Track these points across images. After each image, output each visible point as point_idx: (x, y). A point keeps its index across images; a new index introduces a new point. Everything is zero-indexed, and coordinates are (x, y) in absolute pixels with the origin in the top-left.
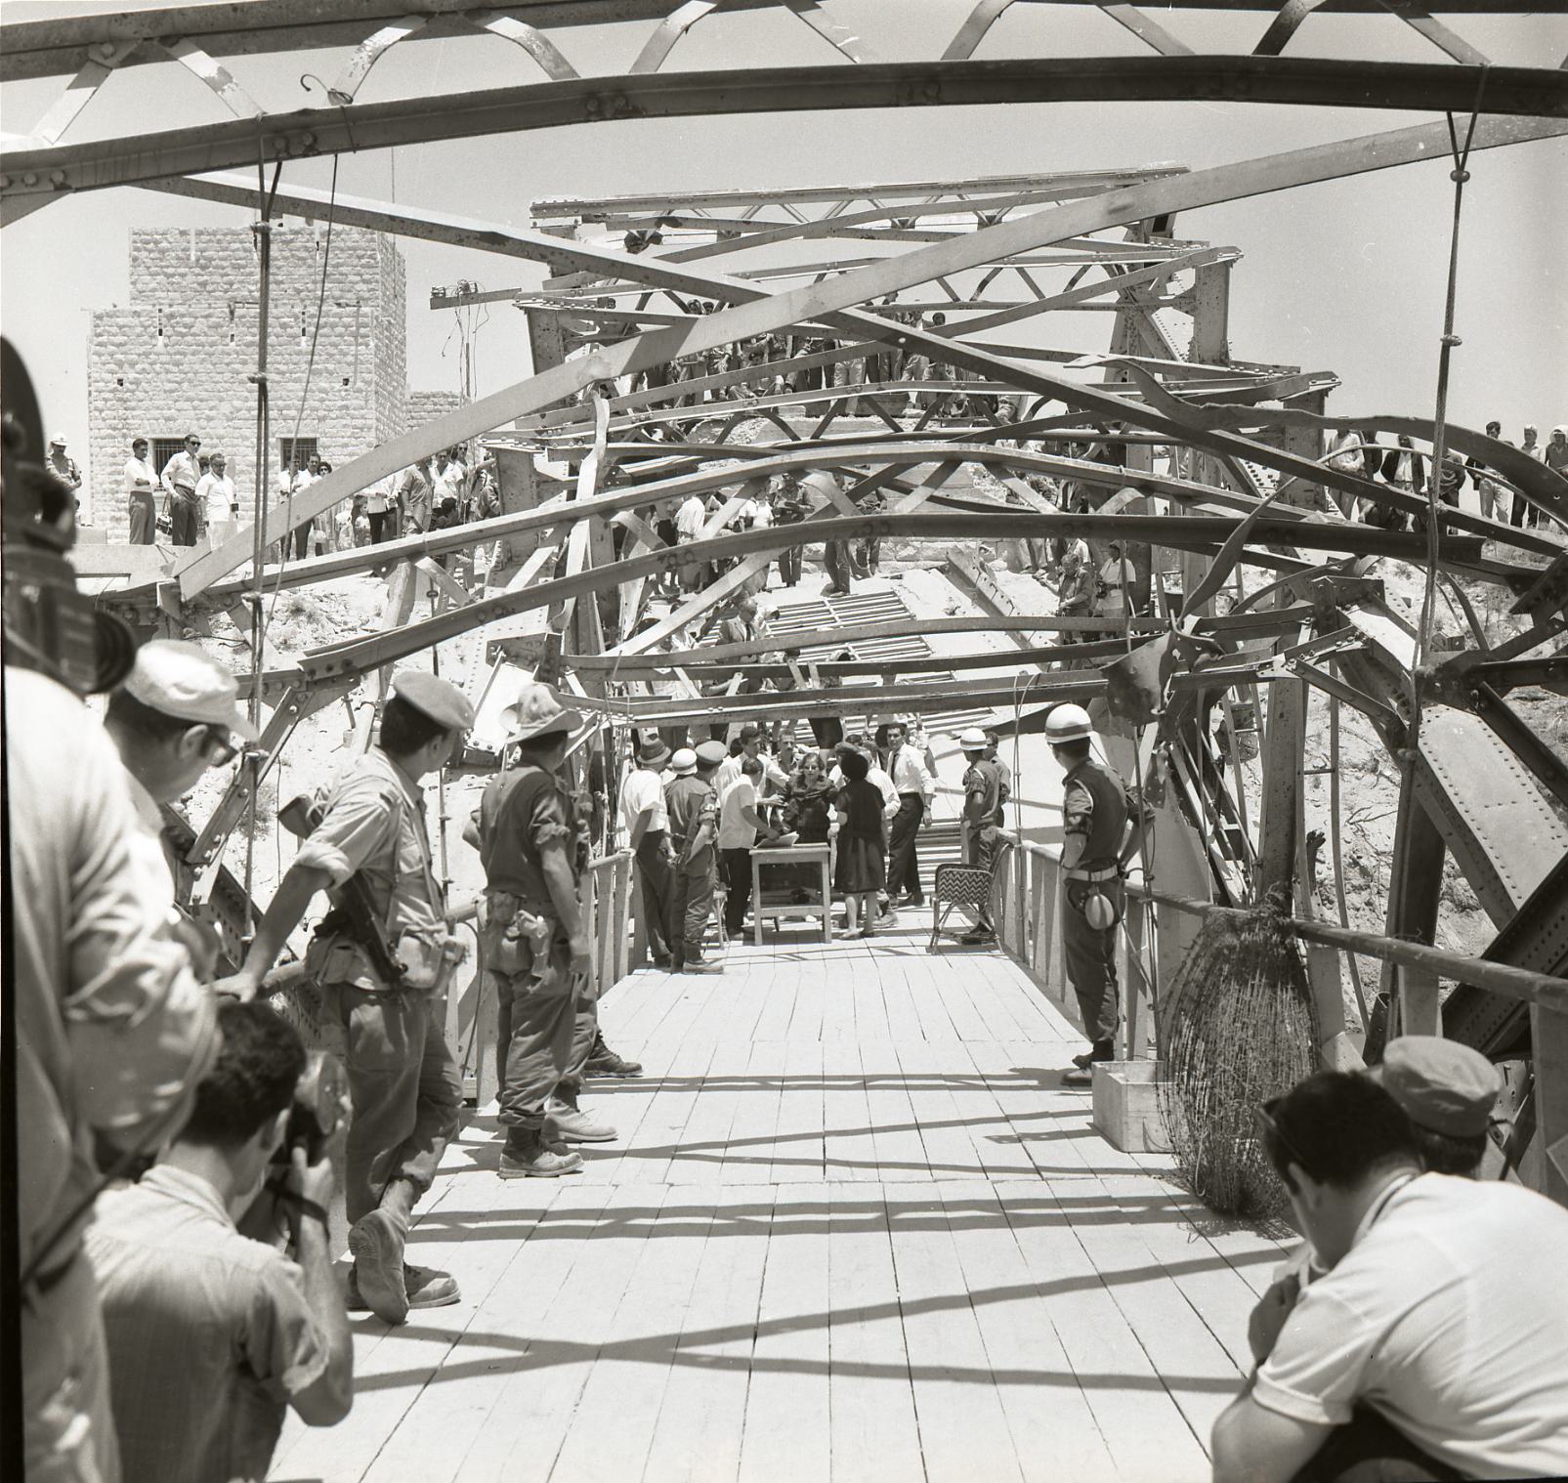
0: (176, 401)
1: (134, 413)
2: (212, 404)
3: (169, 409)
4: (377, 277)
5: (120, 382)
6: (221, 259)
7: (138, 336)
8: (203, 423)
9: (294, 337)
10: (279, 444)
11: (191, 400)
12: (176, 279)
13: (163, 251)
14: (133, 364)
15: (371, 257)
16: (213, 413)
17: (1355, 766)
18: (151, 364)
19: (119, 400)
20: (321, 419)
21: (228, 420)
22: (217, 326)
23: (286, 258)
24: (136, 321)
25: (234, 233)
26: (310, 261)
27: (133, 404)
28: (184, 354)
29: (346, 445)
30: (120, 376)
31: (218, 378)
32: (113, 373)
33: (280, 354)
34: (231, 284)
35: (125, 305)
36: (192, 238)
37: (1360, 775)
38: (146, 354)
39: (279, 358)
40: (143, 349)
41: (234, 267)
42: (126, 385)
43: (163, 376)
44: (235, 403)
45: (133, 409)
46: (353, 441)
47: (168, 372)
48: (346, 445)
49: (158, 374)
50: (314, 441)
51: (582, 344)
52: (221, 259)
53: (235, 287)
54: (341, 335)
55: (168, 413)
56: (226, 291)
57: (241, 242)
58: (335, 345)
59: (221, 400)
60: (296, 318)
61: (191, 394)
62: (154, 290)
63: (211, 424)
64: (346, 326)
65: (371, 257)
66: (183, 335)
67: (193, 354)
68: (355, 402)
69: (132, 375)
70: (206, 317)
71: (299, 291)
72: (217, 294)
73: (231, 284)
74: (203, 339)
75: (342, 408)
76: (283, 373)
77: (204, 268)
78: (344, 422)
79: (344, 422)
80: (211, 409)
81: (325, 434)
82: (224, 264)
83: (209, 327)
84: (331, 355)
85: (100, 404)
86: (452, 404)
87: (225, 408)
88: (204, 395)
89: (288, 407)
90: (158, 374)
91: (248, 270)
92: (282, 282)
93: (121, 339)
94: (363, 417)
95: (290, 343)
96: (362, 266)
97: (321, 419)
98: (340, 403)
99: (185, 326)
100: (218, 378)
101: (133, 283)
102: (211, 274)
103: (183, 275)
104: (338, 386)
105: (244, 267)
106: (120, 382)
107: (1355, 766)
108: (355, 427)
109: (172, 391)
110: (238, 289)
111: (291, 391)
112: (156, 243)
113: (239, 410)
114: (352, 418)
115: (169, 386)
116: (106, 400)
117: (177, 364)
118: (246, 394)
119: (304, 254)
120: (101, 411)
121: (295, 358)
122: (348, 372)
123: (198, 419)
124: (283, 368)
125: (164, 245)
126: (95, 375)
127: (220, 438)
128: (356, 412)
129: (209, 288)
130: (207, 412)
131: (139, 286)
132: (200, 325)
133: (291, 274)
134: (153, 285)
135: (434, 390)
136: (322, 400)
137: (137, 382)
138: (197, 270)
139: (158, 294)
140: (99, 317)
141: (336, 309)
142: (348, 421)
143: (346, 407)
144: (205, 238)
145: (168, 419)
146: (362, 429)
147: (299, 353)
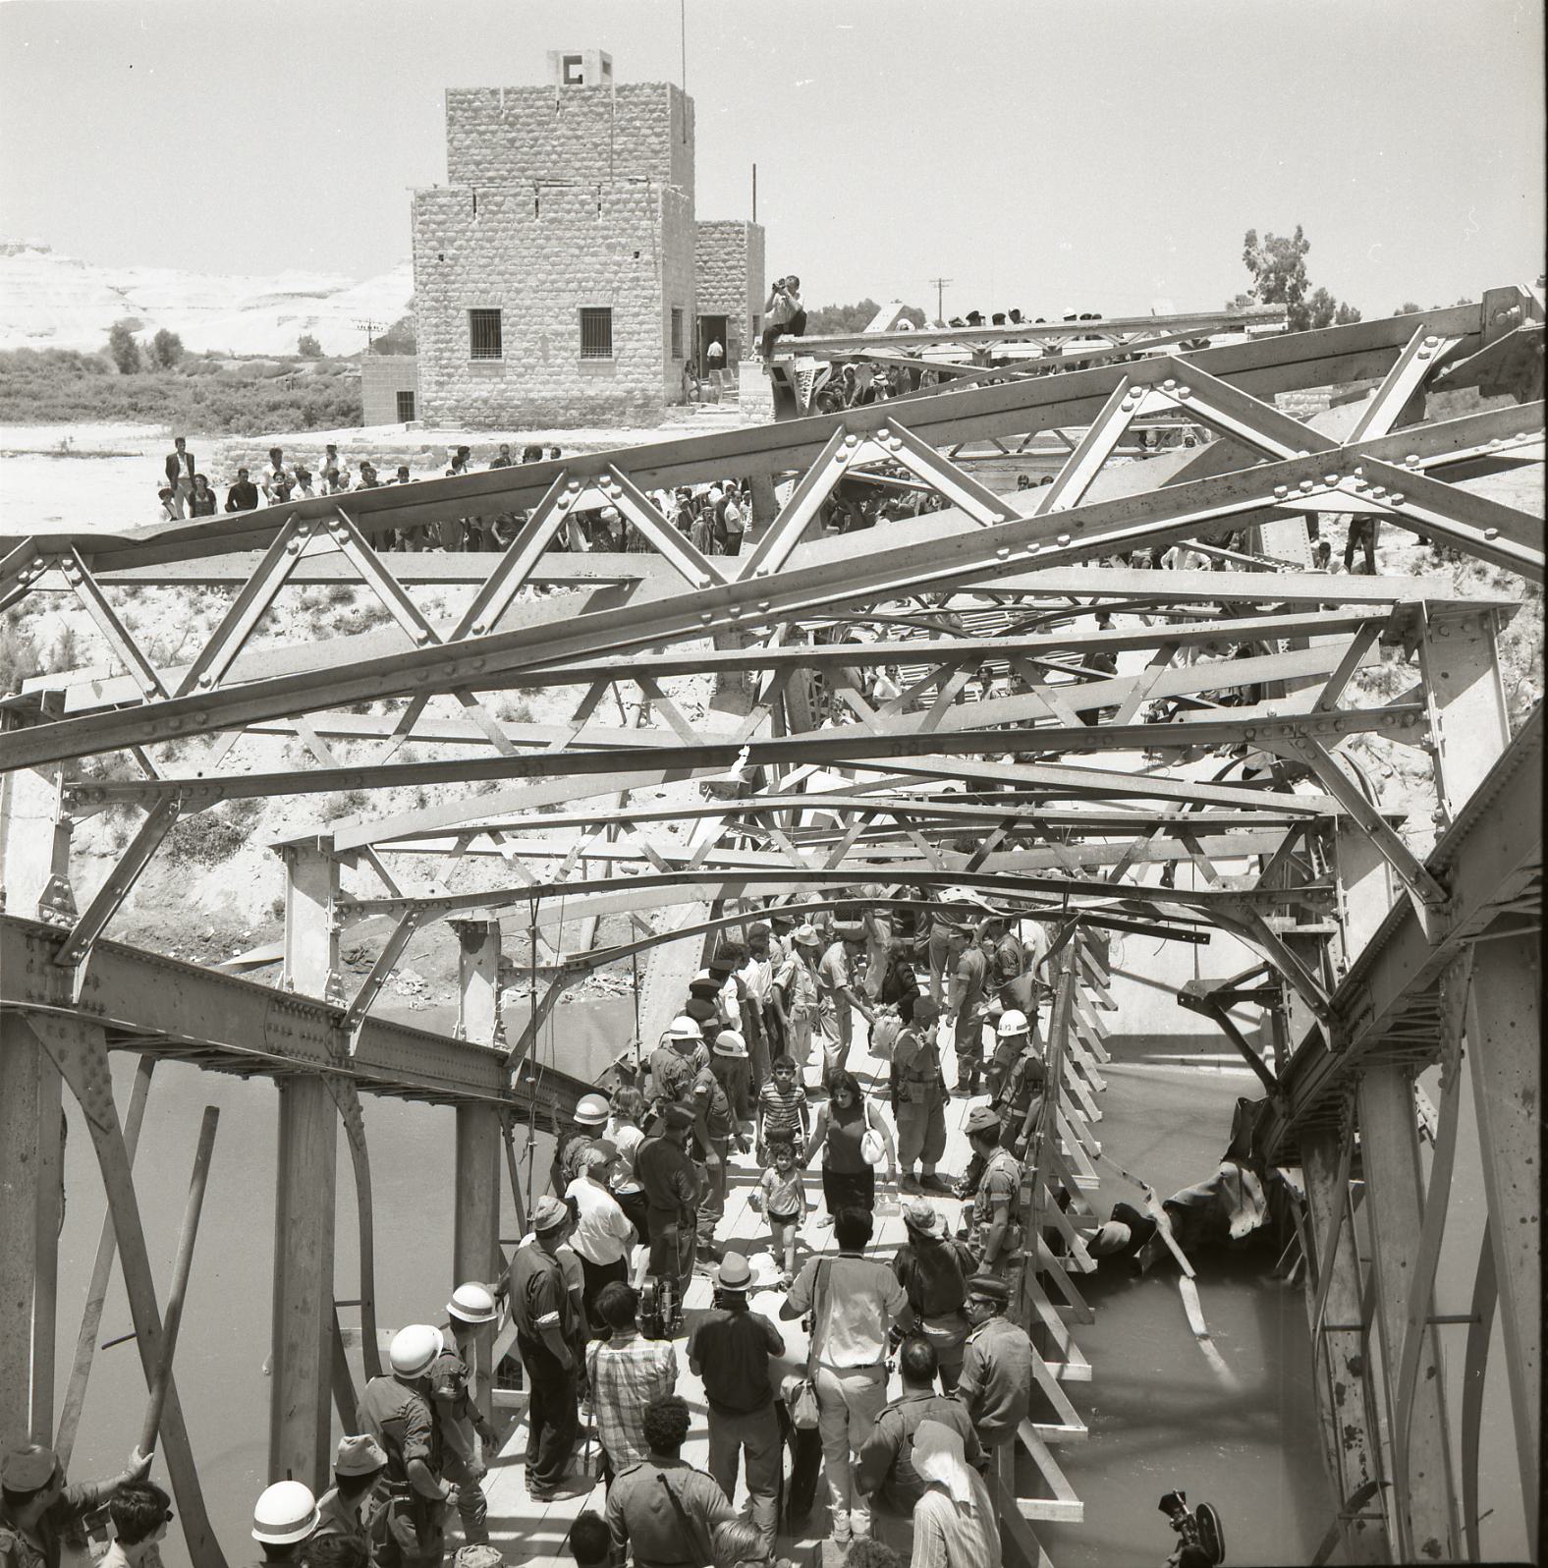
2: (520, 277)
4: (667, 130)
5: (441, 258)
6: (527, 116)
7: (457, 214)
8: (512, 295)
9: (590, 213)
11: (501, 274)
12: (488, 136)
13: (476, 110)
14: (452, 241)
15: (662, 111)
17: (1416, 774)
18: (468, 241)
19: (441, 274)
20: (616, 290)
22: (524, 204)
23: (585, 114)
24: (454, 200)
25: (540, 91)
26: (606, 116)
28: (496, 231)
29: (637, 315)
30: (440, 252)
31: (525, 253)
32: (434, 249)
33: (579, 230)
34: (536, 139)
35: (443, 183)
36: (502, 96)
37: (1419, 782)
38: (463, 232)
39: (577, 234)
40: (460, 226)
41: (540, 124)
42: (446, 260)
43: (477, 252)
46: (643, 311)
47: (482, 248)
48: (637, 315)
49: (473, 250)
50: (609, 310)
51: (787, 479)
52: (527, 116)
53: (541, 141)
54: (632, 211)
55: (482, 286)
56: (532, 147)
57: (545, 99)
58: (627, 220)
59: (528, 274)
60: (593, 195)
61: (502, 268)
62: (468, 147)
63: (521, 295)
64: (637, 202)
65: (662, 111)
66: (494, 213)
67: (504, 230)
68: (644, 274)
69: (451, 252)
70: (515, 195)
71: (596, 145)
72: (525, 149)
73: (536, 139)
74: (511, 216)
75: (633, 280)
76: (581, 248)
77: (512, 125)
81: (617, 304)
82: (530, 120)
83: (518, 205)
84: (624, 230)
85: (424, 278)
86: (738, 232)
87: (532, 282)
90: (473, 250)
91: (551, 126)
92: (581, 137)
93: (442, 217)
95: (587, 219)
96: (654, 120)
97: (616, 290)
98: (631, 275)
99: (496, 205)
100: (525, 253)
101: (451, 141)
102: (519, 131)
103: (493, 133)
104: (630, 259)
105: (548, 123)
106: (441, 258)
107: (1416, 774)
109: (485, 266)
110: (542, 145)
112: (470, 102)
113: (544, 283)
115: (483, 261)
116: (430, 275)
117: (490, 240)
119: (602, 110)
120: (425, 285)
121: (592, 233)
122: (637, 246)
124: (582, 243)
125: (477, 104)
126: (419, 252)
127: (528, 308)
129: (517, 144)
131: (455, 143)
132: (510, 203)
133: (590, 129)
134: (468, 142)
135: (722, 219)
136: (616, 273)
137: (455, 258)
138: (506, 127)
139: (473, 151)
140: (422, 198)
141: (628, 186)
143: (637, 279)
144: (512, 96)
145: (482, 292)
147: (595, 228)
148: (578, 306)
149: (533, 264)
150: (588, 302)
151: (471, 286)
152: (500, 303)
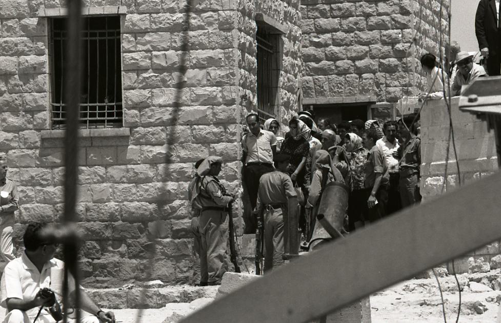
148: (41, 12)
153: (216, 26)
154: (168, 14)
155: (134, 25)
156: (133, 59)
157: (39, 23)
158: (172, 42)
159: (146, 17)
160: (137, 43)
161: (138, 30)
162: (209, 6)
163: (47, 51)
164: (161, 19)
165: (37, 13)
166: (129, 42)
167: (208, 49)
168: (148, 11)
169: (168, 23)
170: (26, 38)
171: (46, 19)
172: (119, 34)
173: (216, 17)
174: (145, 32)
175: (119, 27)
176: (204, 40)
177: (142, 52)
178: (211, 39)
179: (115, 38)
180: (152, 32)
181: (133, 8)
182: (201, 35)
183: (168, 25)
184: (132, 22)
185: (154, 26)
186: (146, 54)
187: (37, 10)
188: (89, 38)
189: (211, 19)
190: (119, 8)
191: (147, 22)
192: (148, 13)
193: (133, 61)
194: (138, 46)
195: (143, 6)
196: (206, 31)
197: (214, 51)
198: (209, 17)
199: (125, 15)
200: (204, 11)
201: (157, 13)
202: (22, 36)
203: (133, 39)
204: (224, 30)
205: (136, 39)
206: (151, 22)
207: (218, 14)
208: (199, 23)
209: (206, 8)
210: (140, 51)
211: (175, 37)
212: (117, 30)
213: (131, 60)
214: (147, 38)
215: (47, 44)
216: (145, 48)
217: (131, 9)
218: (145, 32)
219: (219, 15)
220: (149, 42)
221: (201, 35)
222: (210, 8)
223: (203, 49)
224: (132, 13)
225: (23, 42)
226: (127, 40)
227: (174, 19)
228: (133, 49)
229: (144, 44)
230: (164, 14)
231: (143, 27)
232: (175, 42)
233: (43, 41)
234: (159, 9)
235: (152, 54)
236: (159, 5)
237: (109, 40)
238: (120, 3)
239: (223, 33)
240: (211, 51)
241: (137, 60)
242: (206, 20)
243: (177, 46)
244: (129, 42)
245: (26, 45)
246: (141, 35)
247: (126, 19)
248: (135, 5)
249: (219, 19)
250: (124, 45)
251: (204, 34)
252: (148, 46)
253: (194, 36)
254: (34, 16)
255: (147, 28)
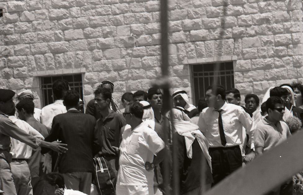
0: (64, 29)
1: (18, 47)
2: (107, 29)
3: (59, 39)
8: (98, 53)
10: (189, 72)
11: (81, 26)
16: (109, 40)
20: (236, 37)
21: (127, 46)
27: (15, 37)
44: (134, 26)
45: (15, 43)
48: (268, 67)
59: (117, 24)
63: (107, 53)
78: (265, 38)
79: (265, 38)
80: (105, 36)
81: (243, 55)
87: (123, 33)
88: (97, 19)
89: (196, 26)
94: (288, 31)
98: (257, 16)
108: (278, 44)
109: (59, 18)
111: (200, 6)
113: (138, 34)
114: (275, 33)
118: (146, 14)
123: (91, 49)
128: (280, 26)
130: (102, 40)
142: (270, 37)
143: (267, 20)
145: (55, 52)
146: (287, 45)
148: (186, 62)
149: (123, 12)
150: (200, 55)
151: (43, 46)
152: (78, 66)
153: (292, 65)
154: (262, 60)
155: (241, 66)
156: (242, 87)
157: (184, 68)
158: (265, 76)
159: (248, 61)
160: (244, 78)
161: (244, 69)
162: (287, 53)
163: (190, 84)
164: (257, 62)
165: (183, 62)
166: (239, 77)
167: (287, 79)
168: (250, 58)
169: (262, 65)
170: (177, 78)
171: (188, 65)
172: (233, 72)
173: (291, 59)
174: (248, 71)
175: (232, 68)
176: (285, 74)
177: (247, 83)
178: (289, 73)
179: (231, 75)
180: (253, 70)
181: (241, 56)
182: (282, 71)
183: (262, 66)
184: (240, 65)
185: (254, 67)
186: (250, 84)
187: (183, 61)
188: (225, 75)
189: (289, 61)
190: (232, 57)
191: (250, 65)
192: (249, 59)
193: (242, 88)
194: (245, 79)
195: (247, 55)
196: (285, 68)
197: (291, 80)
198: (287, 60)
199: (236, 61)
200: (284, 56)
201: (255, 58)
202: (175, 76)
203: (241, 75)
204: (296, 67)
205: (243, 75)
206: (252, 64)
207: (293, 57)
208: (281, 64)
209: (285, 54)
210: (246, 82)
211: (267, 73)
212: (232, 70)
213: (241, 87)
214: (250, 74)
215: (190, 80)
216: (249, 80)
217: (239, 57)
218: (248, 71)
219: (293, 58)
220: (251, 76)
221: (282, 71)
222: (288, 54)
223: (284, 79)
224: (240, 59)
225: (175, 80)
226: (238, 75)
227: (266, 62)
228: (241, 81)
229: (248, 78)
230: (260, 59)
231: (247, 68)
232: (267, 76)
233: (188, 79)
234: (256, 57)
235: (253, 84)
236: (256, 54)
237: (227, 77)
238: (232, 54)
239: (295, 69)
240: (289, 80)
241: (244, 87)
242: (285, 62)
243: (268, 78)
244: (239, 77)
245: (177, 82)
246: (246, 72)
247: (237, 63)
248: (242, 55)
249: (293, 61)
250: (236, 79)
251: (285, 70)
252: (251, 79)
253: (278, 72)
254: (181, 64)
255: (249, 68)
